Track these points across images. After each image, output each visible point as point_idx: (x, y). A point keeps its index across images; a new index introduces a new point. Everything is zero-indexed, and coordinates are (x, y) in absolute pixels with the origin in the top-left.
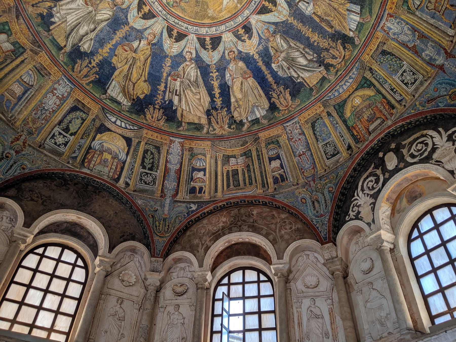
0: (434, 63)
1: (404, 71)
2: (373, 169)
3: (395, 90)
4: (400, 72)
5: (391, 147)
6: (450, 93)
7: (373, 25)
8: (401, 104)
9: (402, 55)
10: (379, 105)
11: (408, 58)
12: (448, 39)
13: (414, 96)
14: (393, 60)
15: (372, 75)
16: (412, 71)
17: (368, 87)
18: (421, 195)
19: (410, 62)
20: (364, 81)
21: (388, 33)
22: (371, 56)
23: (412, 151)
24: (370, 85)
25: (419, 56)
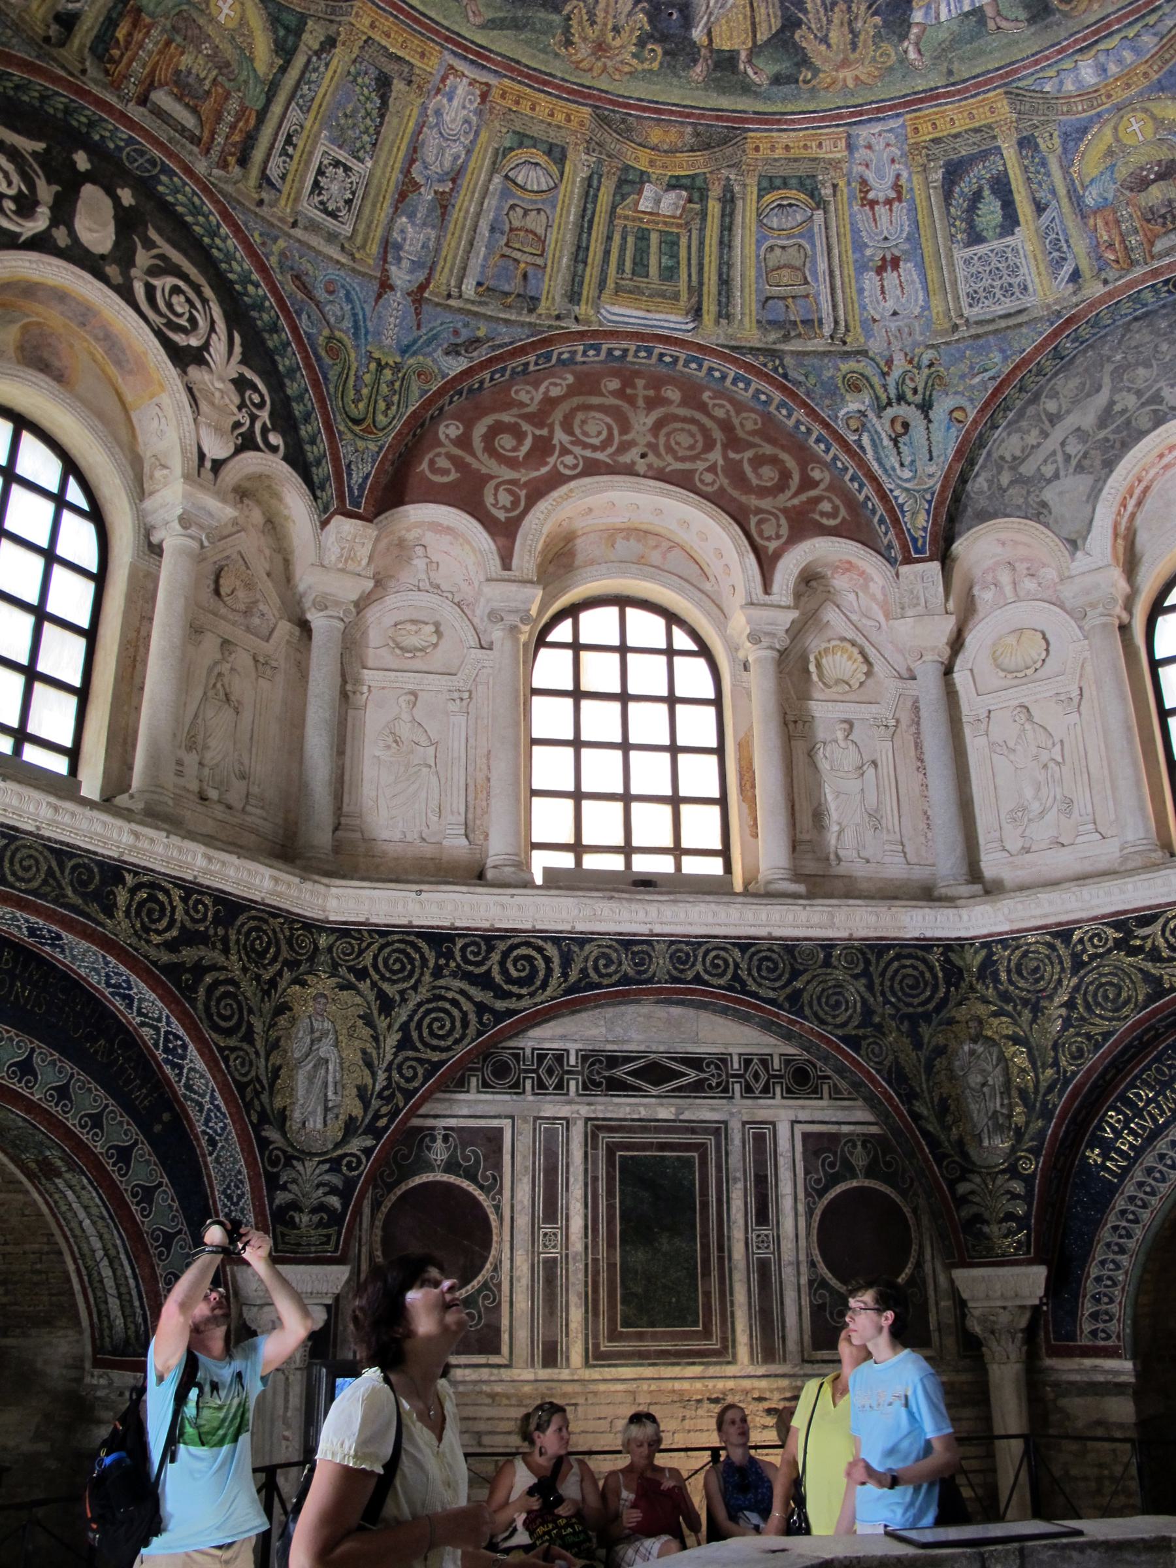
0: (390, 259)
1: (347, 169)
2: (34, 154)
3: (290, 150)
4: (342, 155)
5: (119, 191)
6: (338, 334)
7: (459, 35)
8: (260, 186)
9: (386, 148)
10: (233, 105)
11: (384, 173)
12: (453, 283)
13: (294, 225)
14: (368, 121)
15: (318, 53)
16: (353, 193)
17: (276, 42)
18: (59, 378)
19: (375, 181)
20: (290, 20)
21: (438, 91)
22: (370, 38)
23: (156, 282)
24: (285, 51)
25: (397, 208)
